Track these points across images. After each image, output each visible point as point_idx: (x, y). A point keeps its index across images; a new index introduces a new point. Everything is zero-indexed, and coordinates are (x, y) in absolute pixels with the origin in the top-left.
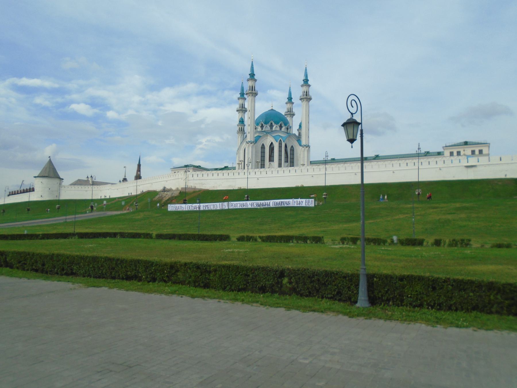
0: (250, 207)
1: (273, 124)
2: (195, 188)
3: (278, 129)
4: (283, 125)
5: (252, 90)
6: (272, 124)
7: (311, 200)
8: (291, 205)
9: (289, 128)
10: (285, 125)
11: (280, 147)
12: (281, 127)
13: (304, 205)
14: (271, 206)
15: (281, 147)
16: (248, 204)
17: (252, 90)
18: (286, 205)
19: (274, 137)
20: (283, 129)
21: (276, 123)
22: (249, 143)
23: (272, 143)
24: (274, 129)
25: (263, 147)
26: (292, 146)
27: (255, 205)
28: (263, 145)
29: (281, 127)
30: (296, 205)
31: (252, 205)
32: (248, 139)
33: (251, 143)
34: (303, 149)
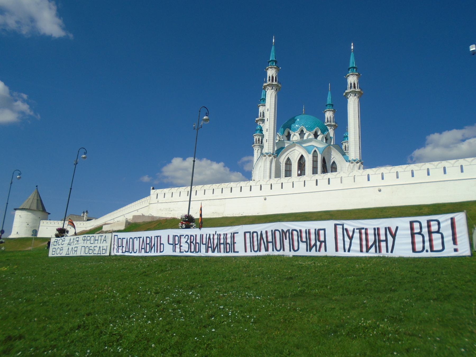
0: (168, 251)
1: (305, 131)
2: (153, 217)
3: (312, 136)
4: (319, 133)
5: (273, 81)
6: (302, 131)
7: (445, 219)
8: (331, 252)
9: (328, 138)
10: (323, 132)
11: (315, 161)
12: (316, 135)
13: (403, 249)
14: (241, 250)
15: (317, 161)
16: (164, 241)
17: (273, 81)
18: (303, 251)
19: (305, 148)
20: (320, 138)
21: (309, 129)
22: (267, 156)
23: (302, 156)
24: (305, 137)
25: (288, 162)
26: (334, 163)
27: (185, 247)
28: (288, 159)
29: (316, 135)
30: (355, 252)
31: (174, 245)
32: (265, 150)
33: (270, 156)
34: (352, 165)
